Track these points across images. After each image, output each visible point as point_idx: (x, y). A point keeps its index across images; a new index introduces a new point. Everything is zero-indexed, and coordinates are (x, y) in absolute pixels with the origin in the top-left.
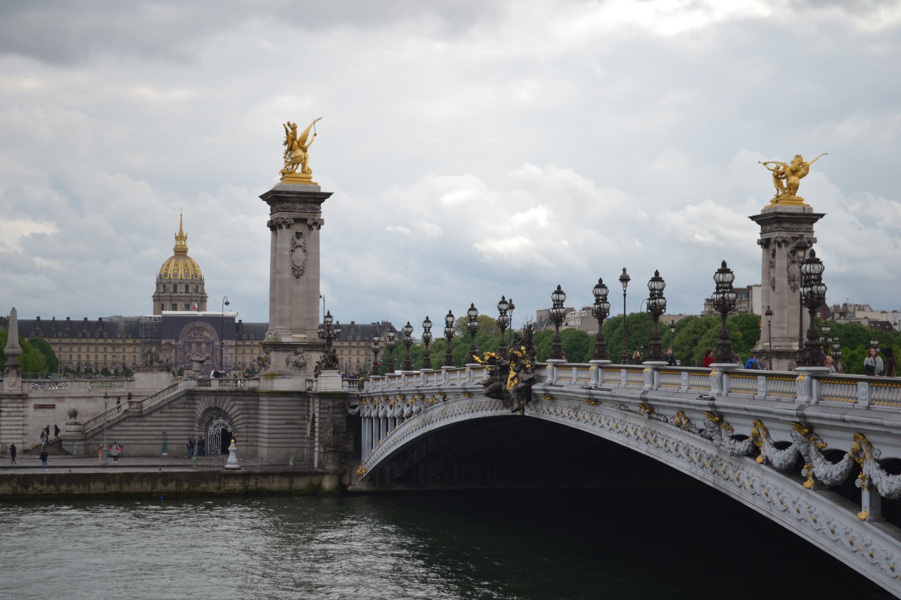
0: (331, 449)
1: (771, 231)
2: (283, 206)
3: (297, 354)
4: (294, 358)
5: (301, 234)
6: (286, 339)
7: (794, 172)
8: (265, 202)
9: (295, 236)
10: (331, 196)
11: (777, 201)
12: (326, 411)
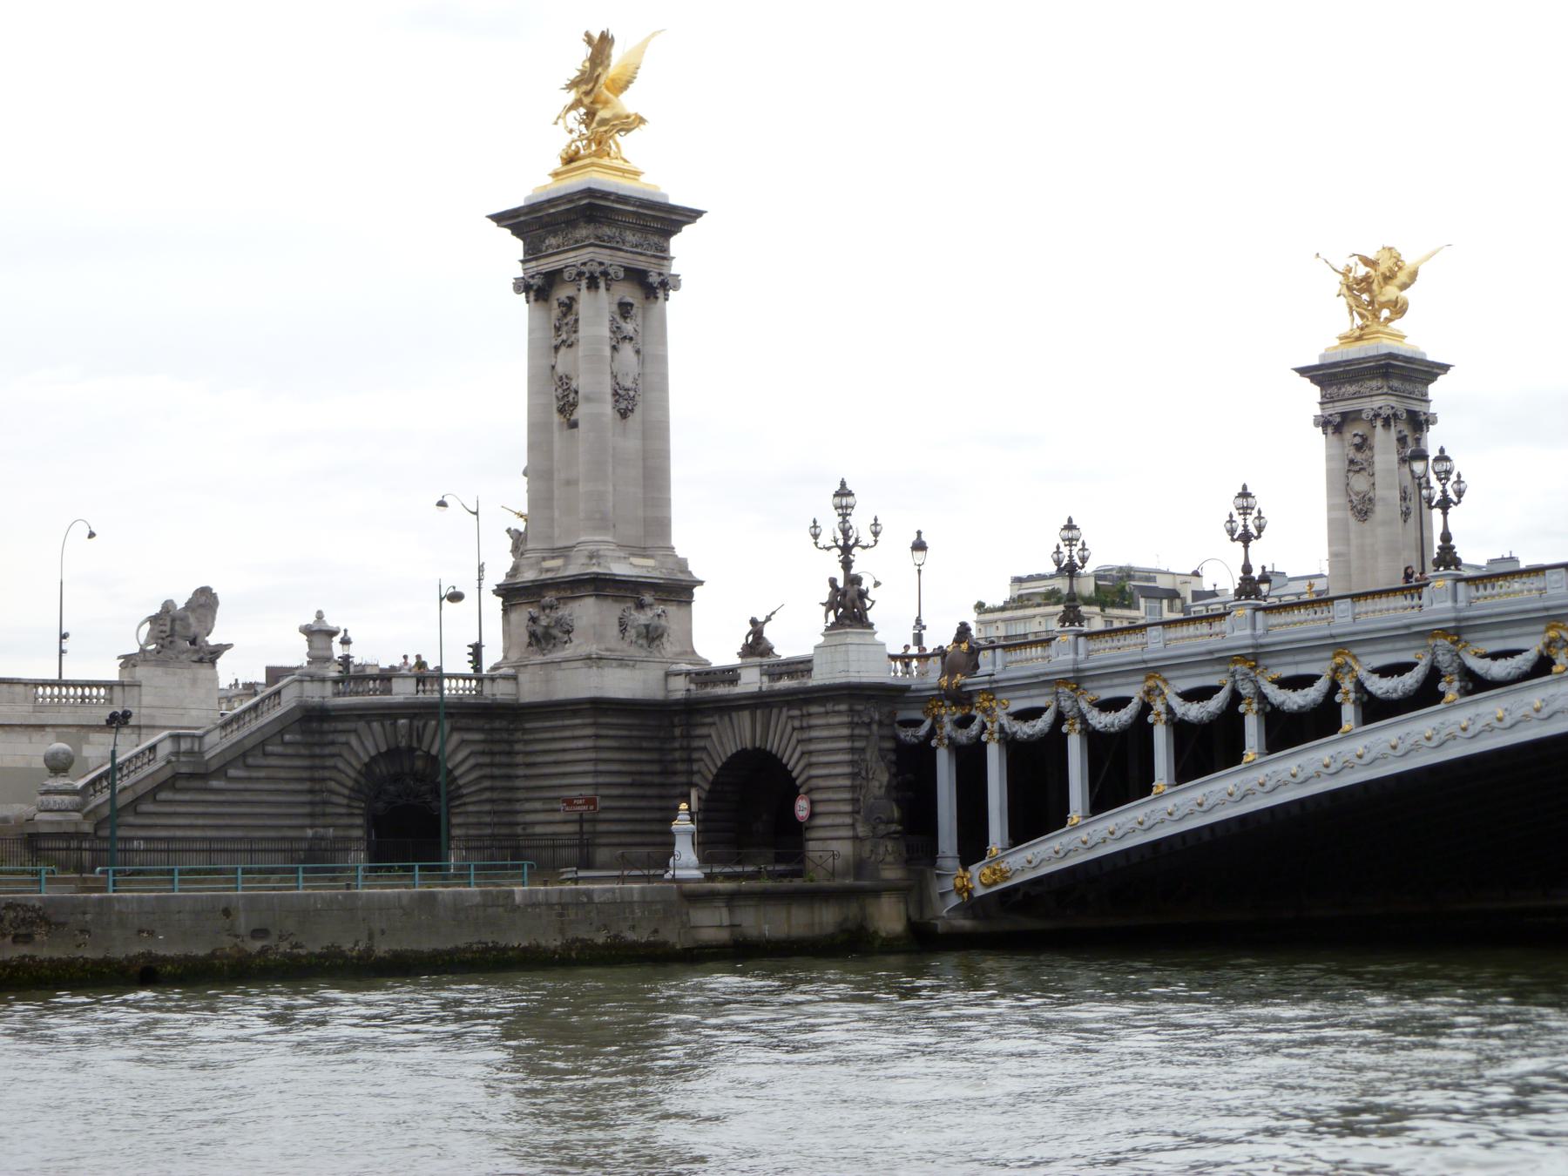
0: (894, 827)
1: (1357, 396)
2: (600, 232)
3: (641, 606)
4: (643, 618)
5: (631, 305)
6: (620, 569)
7: (1388, 278)
8: (508, 231)
9: (618, 312)
10: (699, 220)
11: (1359, 338)
12: (864, 732)
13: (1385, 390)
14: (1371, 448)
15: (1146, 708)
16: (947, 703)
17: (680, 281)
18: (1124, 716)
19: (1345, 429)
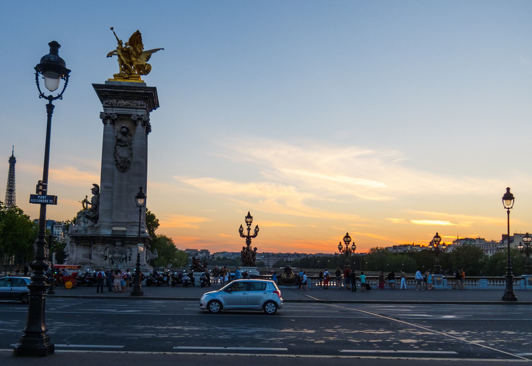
13: (145, 107)
19: (116, 123)
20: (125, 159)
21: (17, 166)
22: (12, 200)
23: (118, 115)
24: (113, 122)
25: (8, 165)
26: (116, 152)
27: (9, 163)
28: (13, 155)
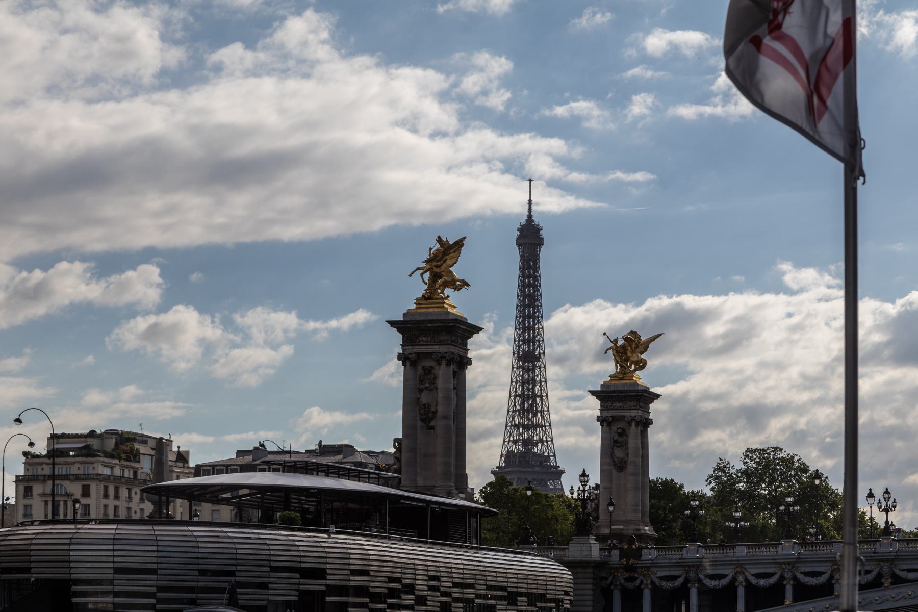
11: (622, 379)
14: (627, 436)
15: (734, 579)
16: (621, 570)
17: (471, 361)
18: (724, 582)
20: (622, 459)
21: (545, 253)
22: (535, 396)
23: (613, 417)
24: (609, 424)
25: (514, 256)
26: (613, 452)
27: (516, 248)
28: (530, 216)
